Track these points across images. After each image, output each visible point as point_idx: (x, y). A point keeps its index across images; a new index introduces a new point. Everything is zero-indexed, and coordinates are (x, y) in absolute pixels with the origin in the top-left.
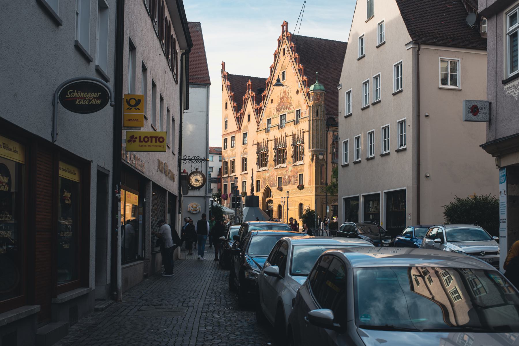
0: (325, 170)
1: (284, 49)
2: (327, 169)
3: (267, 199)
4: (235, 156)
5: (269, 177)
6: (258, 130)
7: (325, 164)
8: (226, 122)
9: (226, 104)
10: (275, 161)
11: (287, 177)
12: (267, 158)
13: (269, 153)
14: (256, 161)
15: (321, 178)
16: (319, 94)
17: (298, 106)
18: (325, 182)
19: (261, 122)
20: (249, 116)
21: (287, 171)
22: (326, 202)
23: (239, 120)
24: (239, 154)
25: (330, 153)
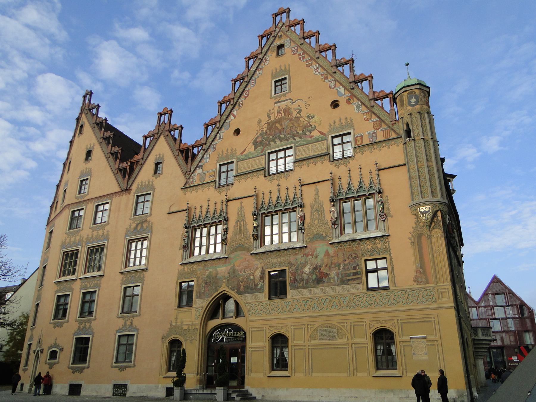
1: (281, 47)
5: (233, 272)
9: (89, 153)
11: (307, 269)
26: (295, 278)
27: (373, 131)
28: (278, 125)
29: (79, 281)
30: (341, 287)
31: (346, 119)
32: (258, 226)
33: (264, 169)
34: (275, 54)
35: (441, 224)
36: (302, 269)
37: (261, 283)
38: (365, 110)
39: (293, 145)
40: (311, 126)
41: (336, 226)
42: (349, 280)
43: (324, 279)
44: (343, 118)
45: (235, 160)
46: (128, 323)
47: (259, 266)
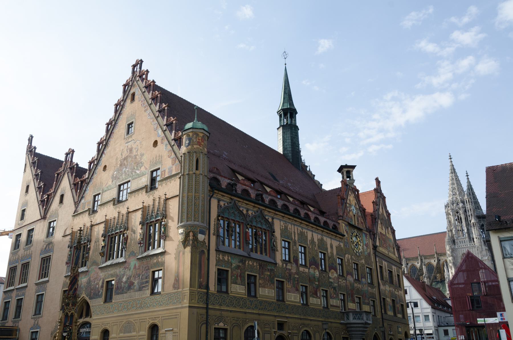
0: (206, 261)
1: (133, 95)
2: (208, 259)
3: (81, 321)
4: (31, 257)
5: (89, 282)
6: (76, 214)
7: (206, 252)
8: (24, 211)
9: (28, 187)
10: (102, 254)
11: (124, 279)
12: (88, 253)
13: (93, 243)
14: (65, 259)
15: (200, 277)
16: (201, 135)
17: (156, 163)
18: (204, 283)
19: (83, 201)
20: (62, 196)
21: (125, 268)
22: (207, 320)
23: (45, 204)
24: (38, 252)
25: (214, 234)
26: (118, 287)
27: (171, 165)
28: (125, 162)
29: (15, 291)
30: (139, 292)
31: (159, 156)
32: (105, 245)
33: (114, 200)
34: (130, 101)
35: (191, 242)
36: (122, 279)
37: (101, 291)
38: (169, 148)
39: (130, 179)
40: (141, 163)
41: (142, 245)
42: (143, 287)
43: (132, 287)
44: (158, 155)
45: (101, 192)
46: (36, 323)
47: (102, 277)
